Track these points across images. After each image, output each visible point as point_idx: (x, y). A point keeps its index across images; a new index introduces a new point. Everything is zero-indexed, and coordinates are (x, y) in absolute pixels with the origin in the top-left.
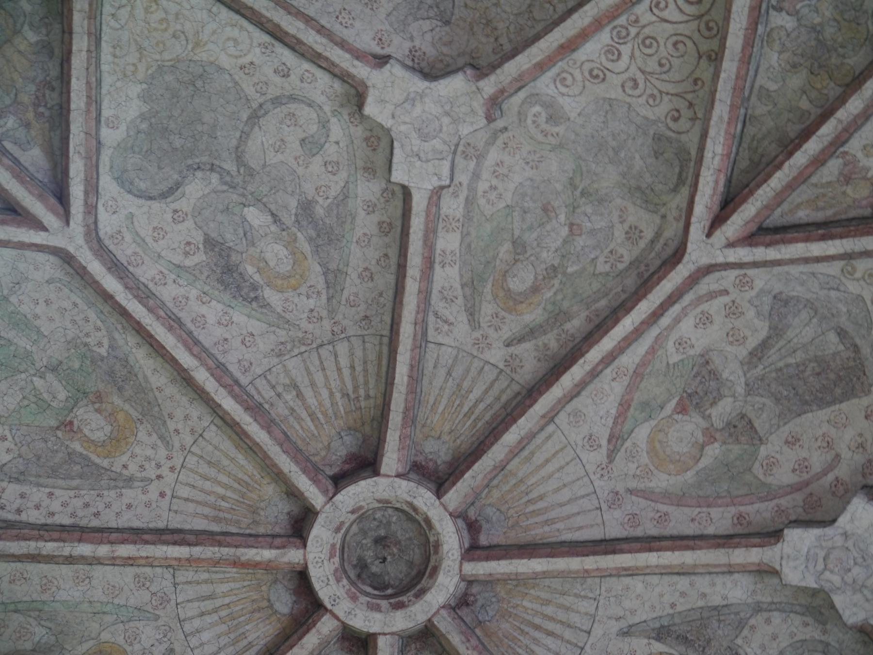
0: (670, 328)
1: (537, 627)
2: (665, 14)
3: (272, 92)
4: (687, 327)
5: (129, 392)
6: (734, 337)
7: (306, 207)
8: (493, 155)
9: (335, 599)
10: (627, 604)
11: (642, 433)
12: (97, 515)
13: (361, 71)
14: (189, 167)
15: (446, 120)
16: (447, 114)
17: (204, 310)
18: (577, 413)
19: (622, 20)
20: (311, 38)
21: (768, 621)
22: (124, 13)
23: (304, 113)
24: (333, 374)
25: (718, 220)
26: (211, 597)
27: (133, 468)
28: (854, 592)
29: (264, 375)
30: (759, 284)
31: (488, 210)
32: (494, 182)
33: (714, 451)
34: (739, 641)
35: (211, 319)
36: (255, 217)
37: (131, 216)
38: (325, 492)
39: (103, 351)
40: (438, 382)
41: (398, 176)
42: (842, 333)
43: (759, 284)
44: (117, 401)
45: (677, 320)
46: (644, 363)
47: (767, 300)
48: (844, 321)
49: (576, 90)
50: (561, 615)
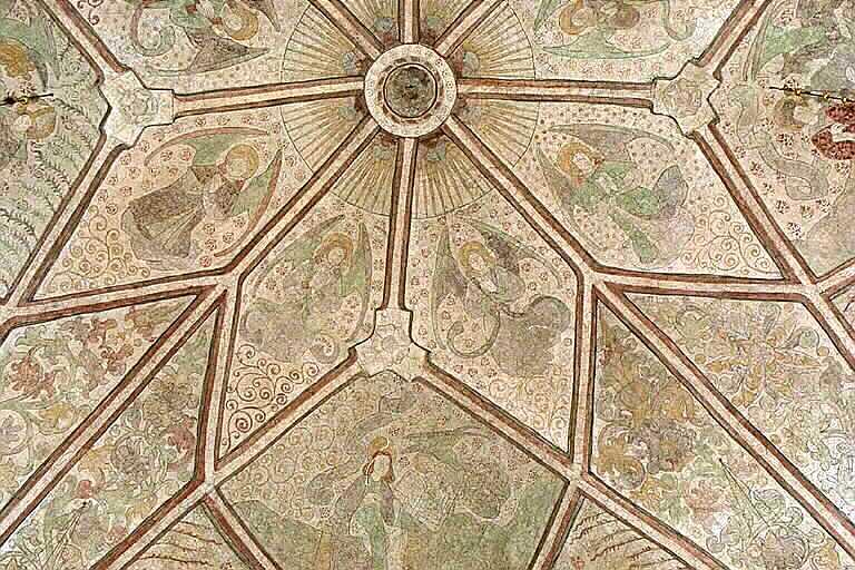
0: (247, 233)
1: (317, 50)
2: (257, 412)
3: (479, 359)
4: (238, 233)
5: (563, 183)
6: (210, 229)
7: (461, 292)
8: (354, 325)
9: (438, 62)
10: (266, 68)
11: (262, 169)
12: (580, 110)
13: (426, 375)
14: (527, 315)
15: (379, 348)
16: (379, 352)
17: (519, 232)
18: (301, 179)
19: (281, 407)
20: (455, 394)
21: (181, 64)
22: (560, 404)
23: (460, 347)
24: (445, 195)
25: (222, 298)
26: (511, 61)
27: (560, 137)
28: (129, 91)
29: (485, 193)
30: (197, 261)
31: (356, 294)
32: (352, 311)
33: (220, 161)
34: (197, 50)
35: (515, 226)
36: (489, 286)
37: (560, 287)
38: (446, 127)
39: (577, 207)
40: (382, 193)
41: (407, 315)
42: (148, 236)
43: (197, 261)
44: (569, 177)
45: (243, 237)
46: (262, 211)
47: (192, 253)
48: (147, 243)
49: (307, 366)
50: (304, 58)
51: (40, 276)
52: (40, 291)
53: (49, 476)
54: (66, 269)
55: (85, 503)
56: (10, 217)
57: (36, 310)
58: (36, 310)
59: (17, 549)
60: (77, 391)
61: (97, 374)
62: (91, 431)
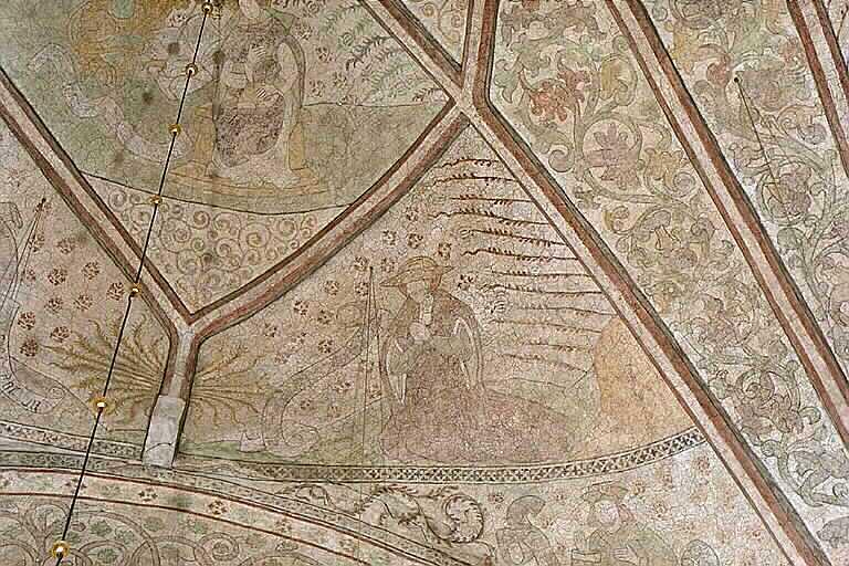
51: (433, 48)
52: (454, 53)
53: (681, 115)
54: (436, 13)
55: (736, 80)
56: (358, 59)
57: (472, 67)
58: (472, 67)
59: (757, 178)
60: (594, 45)
61: (579, 13)
62: (645, 47)
